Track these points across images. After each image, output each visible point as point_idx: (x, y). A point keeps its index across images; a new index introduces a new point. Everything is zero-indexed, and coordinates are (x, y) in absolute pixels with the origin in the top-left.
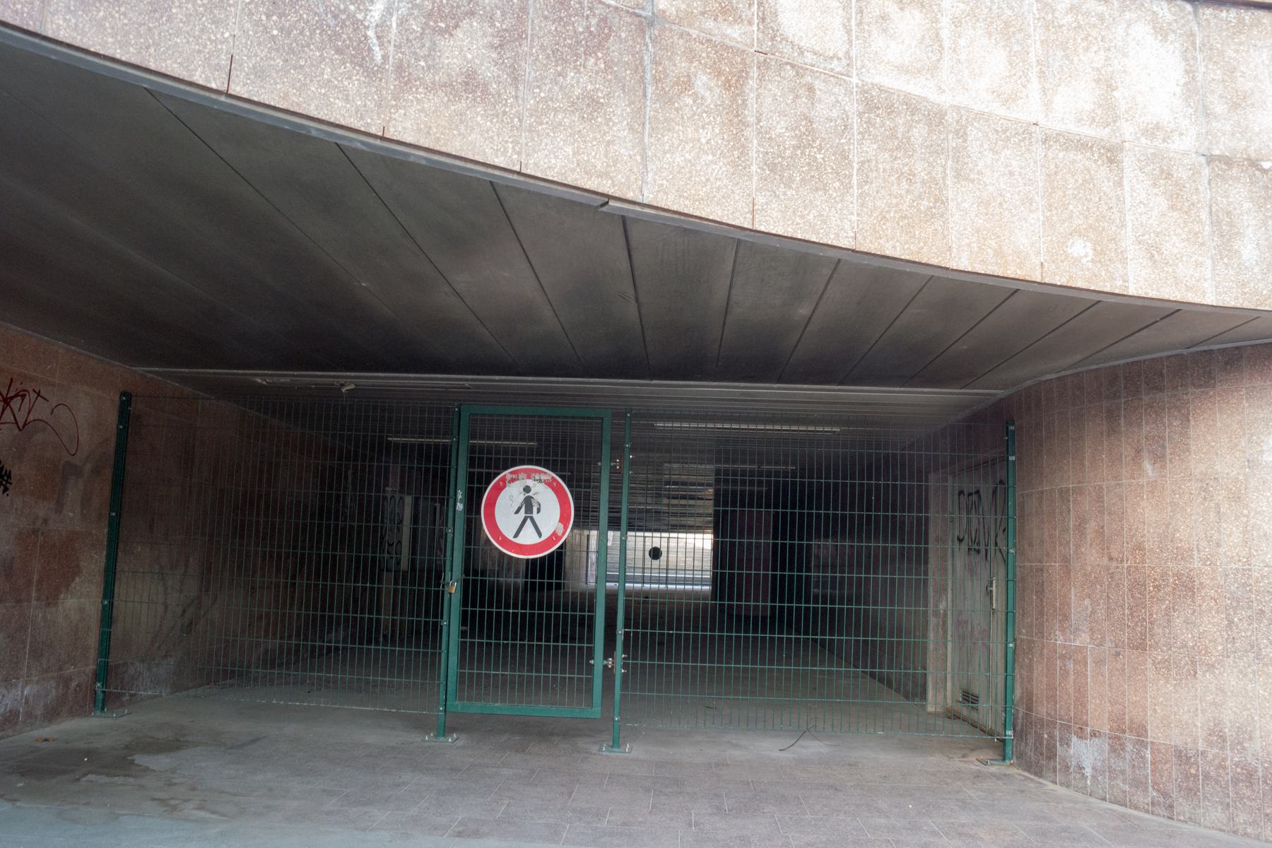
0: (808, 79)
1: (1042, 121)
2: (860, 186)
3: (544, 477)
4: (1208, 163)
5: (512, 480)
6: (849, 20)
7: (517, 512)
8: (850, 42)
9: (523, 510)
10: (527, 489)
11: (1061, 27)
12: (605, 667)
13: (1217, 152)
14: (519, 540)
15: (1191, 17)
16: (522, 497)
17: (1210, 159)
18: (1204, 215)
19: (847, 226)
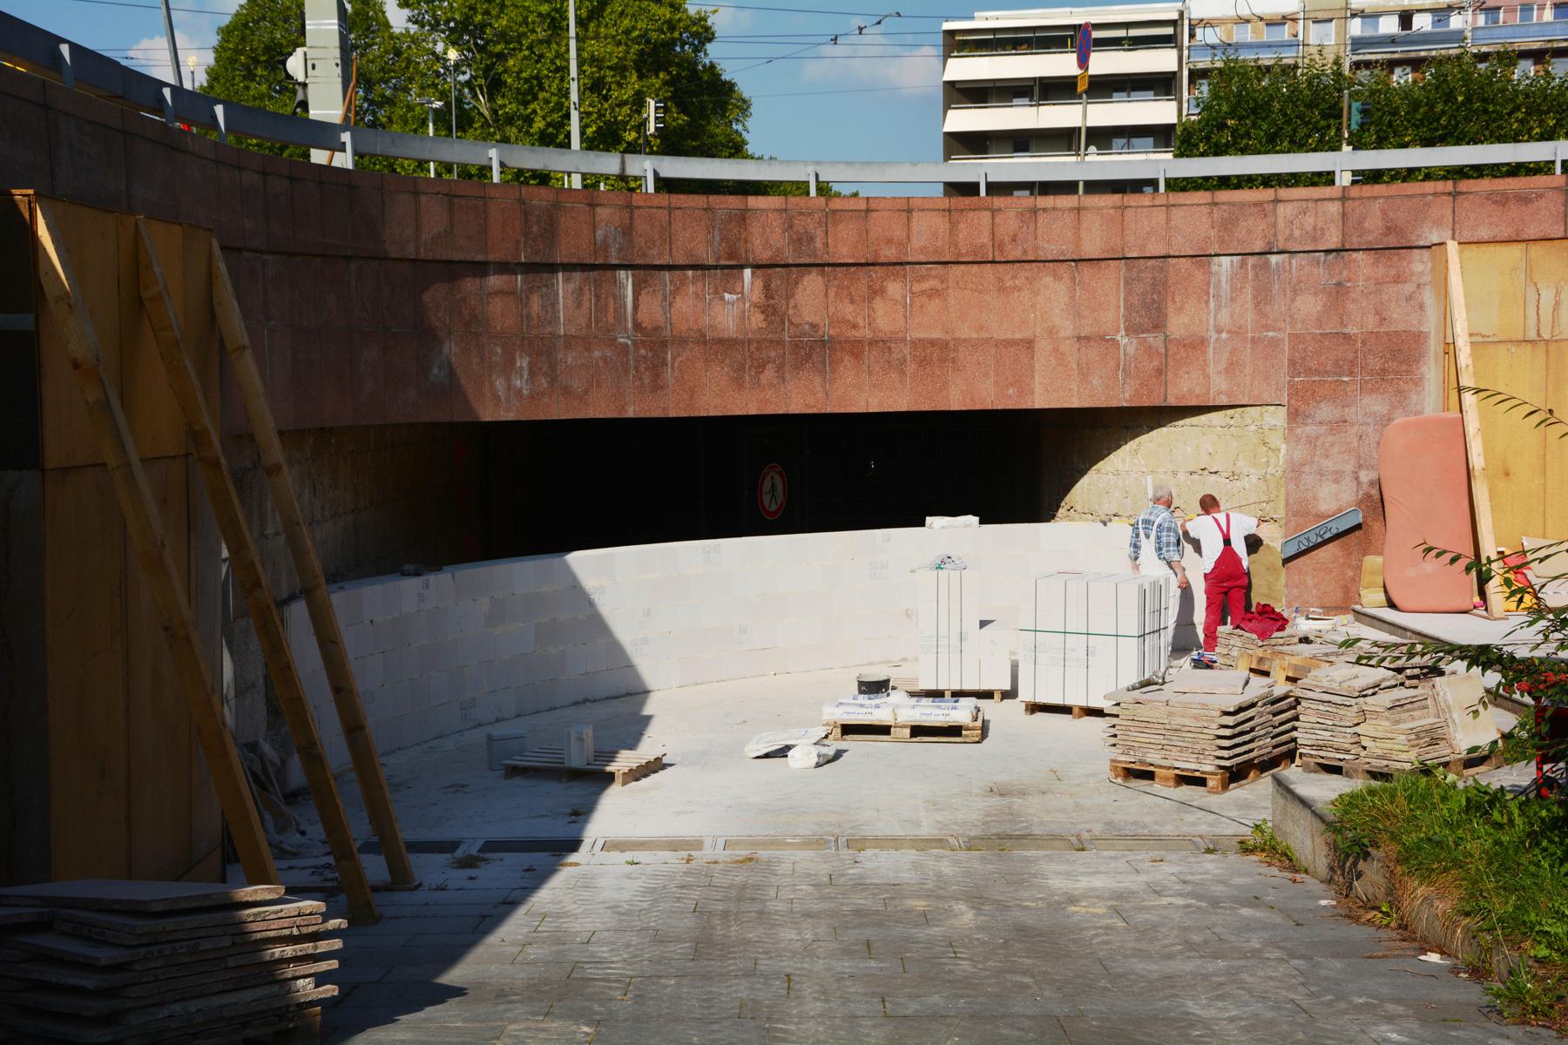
13: (1083, 335)
18: (1075, 366)
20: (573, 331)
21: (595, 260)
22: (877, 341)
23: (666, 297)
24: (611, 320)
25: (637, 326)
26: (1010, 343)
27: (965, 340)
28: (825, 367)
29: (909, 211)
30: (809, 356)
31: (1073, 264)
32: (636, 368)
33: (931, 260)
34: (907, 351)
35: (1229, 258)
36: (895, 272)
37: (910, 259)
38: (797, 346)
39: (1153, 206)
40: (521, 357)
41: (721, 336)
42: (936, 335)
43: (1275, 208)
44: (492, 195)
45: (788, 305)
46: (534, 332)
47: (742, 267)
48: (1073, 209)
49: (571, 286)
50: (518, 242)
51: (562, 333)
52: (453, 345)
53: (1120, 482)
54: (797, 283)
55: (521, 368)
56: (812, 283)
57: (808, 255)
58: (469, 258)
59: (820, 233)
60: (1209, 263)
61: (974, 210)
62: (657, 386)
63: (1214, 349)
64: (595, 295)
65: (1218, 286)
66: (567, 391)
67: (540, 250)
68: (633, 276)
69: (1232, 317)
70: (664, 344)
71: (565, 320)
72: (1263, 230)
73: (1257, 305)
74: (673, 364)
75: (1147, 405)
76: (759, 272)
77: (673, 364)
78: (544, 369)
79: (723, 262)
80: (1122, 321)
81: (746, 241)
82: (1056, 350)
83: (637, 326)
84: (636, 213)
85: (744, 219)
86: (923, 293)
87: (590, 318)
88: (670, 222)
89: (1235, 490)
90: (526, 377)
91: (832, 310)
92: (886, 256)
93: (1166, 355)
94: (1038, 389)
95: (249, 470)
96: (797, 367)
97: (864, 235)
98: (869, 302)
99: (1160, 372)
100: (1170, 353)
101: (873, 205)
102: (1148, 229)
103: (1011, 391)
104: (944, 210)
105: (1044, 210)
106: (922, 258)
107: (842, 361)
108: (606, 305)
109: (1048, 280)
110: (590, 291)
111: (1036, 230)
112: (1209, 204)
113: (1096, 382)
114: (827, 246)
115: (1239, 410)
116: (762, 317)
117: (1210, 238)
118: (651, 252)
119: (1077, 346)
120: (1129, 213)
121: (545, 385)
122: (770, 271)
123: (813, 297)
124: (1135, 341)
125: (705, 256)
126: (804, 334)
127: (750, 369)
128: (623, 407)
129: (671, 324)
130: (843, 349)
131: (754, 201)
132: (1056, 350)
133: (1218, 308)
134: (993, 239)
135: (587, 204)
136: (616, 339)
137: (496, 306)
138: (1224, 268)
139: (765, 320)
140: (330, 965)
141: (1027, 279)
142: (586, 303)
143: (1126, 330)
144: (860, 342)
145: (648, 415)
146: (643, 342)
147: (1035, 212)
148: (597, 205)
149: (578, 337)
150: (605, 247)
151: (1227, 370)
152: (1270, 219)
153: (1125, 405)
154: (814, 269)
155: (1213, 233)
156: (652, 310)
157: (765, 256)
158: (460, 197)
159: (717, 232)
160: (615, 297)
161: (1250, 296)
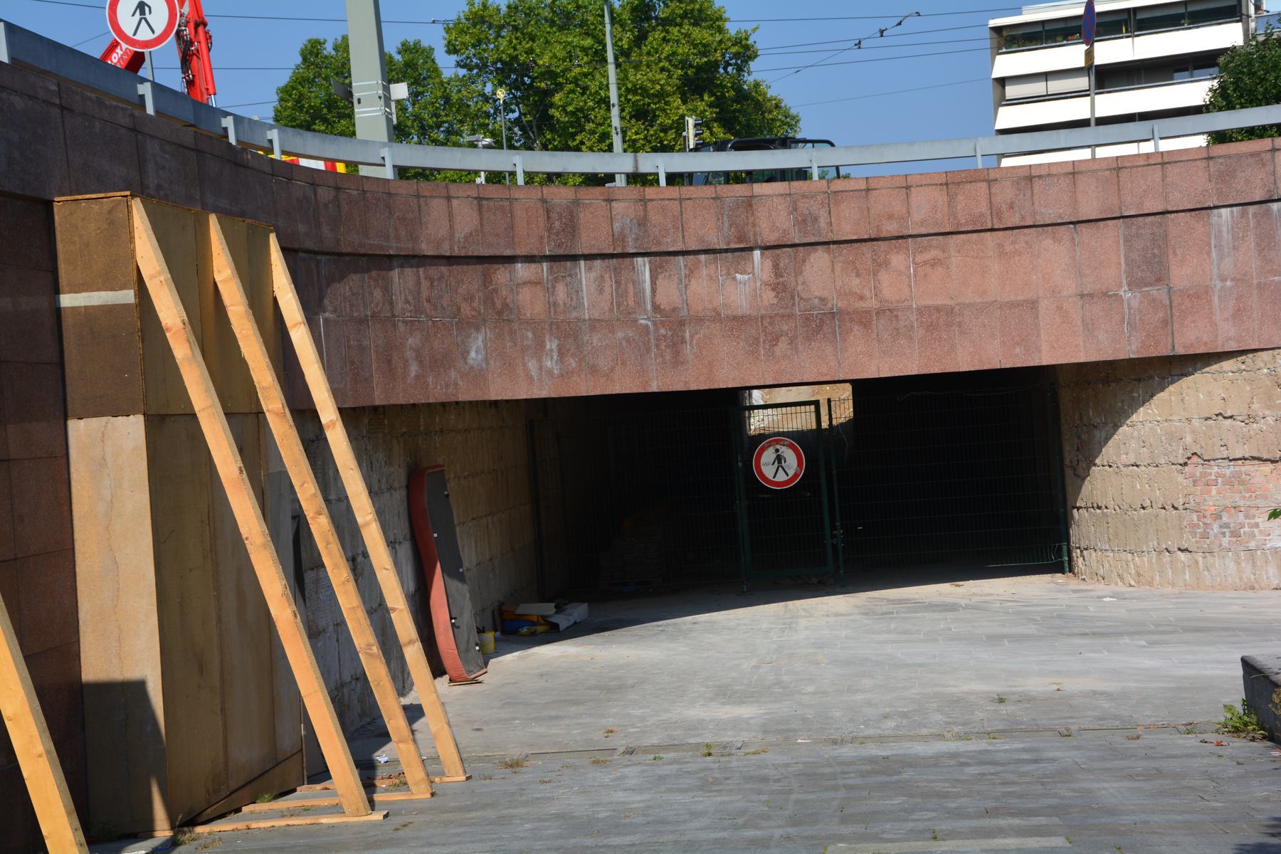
0: (895, 313)
1: (999, 299)
2: (919, 349)
3: (786, 443)
4: (1081, 298)
5: (770, 446)
6: (911, 282)
7: (773, 464)
8: (911, 291)
9: (776, 462)
10: (777, 451)
11: (1006, 253)
12: (833, 544)
13: (1086, 292)
14: (777, 479)
15: (1073, 230)
16: (775, 456)
17: (1082, 296)
18: (1079, 323)
19: (914, 366)
20: (596, 316)
21: (614, 249)
22: (884, 311)
23: (681, 281)
24: (631, 303)
25: (656, 308)
26: (1013, 305)
27: (969, 304)
28: (835, 337)
29: (908, 188)
30: (819, 328)
31: (1072, 226)
32: (657, 346)
33: (932, 232)
34: (913, 318)
35: (1229, 209)
36: (897, 245)
37: (911, 232)
38: (808, 319)
39: (1148, 165)
40: (550, 341)
41: (735, 313)
42: (941, 301)
43: (1273, 157)
44: (516, 197)
45: (797, 281)
46: (561, 318)
47: (751, 249)
48: (1069, 173)
49: (593, 275)
50: (542, 238)
51: (587, 317)
52: (488, 332)
53: (1136, 433)
54: (804, 261)
55: (551, 350)
56: (819, 258)
57: (814, 235)
58: (498, 253)
59: (823, 214)
60: (1209, 216)
61: (971, 182)
62: (677, 361)
63: (1219, 297)
64: (616, 283)
65: (1219, 236)
66: (594, 370)
67: (563, 243)
68: (650, 262)
69: (1235, 266)
70: (682, 323)
71: (589, 305)
72: (1262, 179)
73: (1261, 251)
74: (691, 341)
75: (1154, 355)
76: (767, 252)
77: (691, 341)
78: (572, 350)
79: (733, 246)
80: (1124, 276)
81: (754, 225)
82: (1059, 308)
83: (656, 308)
84: (650, 205)
85: (751, 205)
86: (925, 263)
87: (612, 303)
88: (681, 212)
89: (1252, 433)
90: (555, 358)
91: (839, 284)
92: (887, 231)
93: (1171, 306)
94: (1045, 347)
95: (313, 441)
96: (809, 339)
97: (866, 213)
98: (874, 275)
99: (1165, 323)
100: (1175, 304)
101: (872, 185)
102: (1144, 187)
103: (1018, 350)
104: (941, 184)
105: (1040, 177)
106: (923, 231)
107: (852, 331)
108: (626, 291)
109: (1048, 243)
110: (611, 278)
111: (1032, 196)
112: (1205, 158)
113: (1102, 336)
114: (831, 225)
115: (1250, 355)
116: (773, 294)
117: (1207, 191)
118: (665, 240)
119: (1080, 303)
120: (1124, 173)
121: (574, 365)
122: (778, 251)
123: (820, 273)
124: (1139, 295)
125: (716, 240)
126: (814, 308)
127: (764, 342)
128: (647, 382)
129: (687, 304)
130: (852, 320)
131: (760, 188)
132: (1059, 308)
133: (1221, 258)
134: (991, 208)
135: (604, 200)
136: (637, 321)
137: (525, 295)
138: (1224, 218)
139: (776, 297)
140: (336, 566)
141: (1027, 243)
142: (607, 290)
143: (1129, 285)
144: (868, 312)
145: (671, 389)
146: (662, 322)
147: (1031, 180)
148: (613, 200)
149: (602, 320)
150: (622, 238)
151: (1234, 316)
152: (1269, 168)
153: (1132, 356)
154: (820, 247)
155: (1210, 186)
156: (669, 293)
157: (772, 238)
158: (487, 199)
159: (725, 218)
160: (634, 282)
161: (1253, 245)
